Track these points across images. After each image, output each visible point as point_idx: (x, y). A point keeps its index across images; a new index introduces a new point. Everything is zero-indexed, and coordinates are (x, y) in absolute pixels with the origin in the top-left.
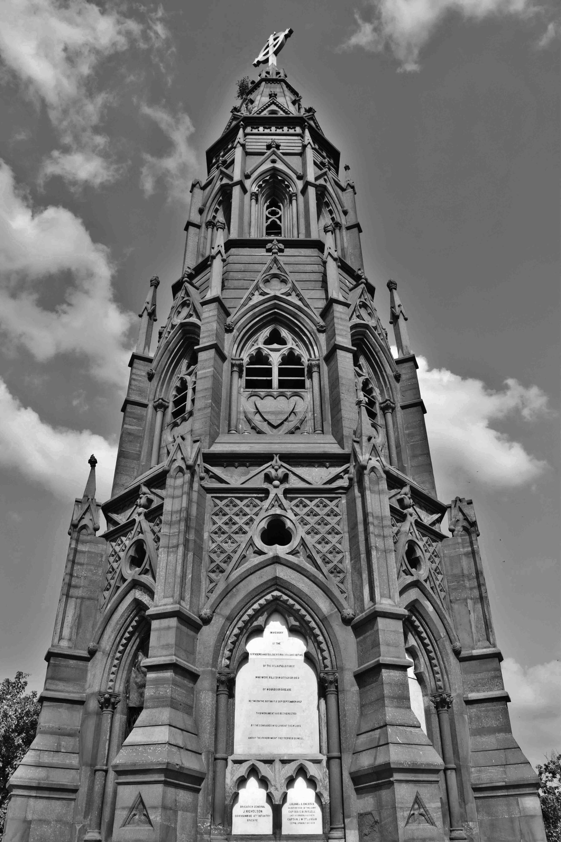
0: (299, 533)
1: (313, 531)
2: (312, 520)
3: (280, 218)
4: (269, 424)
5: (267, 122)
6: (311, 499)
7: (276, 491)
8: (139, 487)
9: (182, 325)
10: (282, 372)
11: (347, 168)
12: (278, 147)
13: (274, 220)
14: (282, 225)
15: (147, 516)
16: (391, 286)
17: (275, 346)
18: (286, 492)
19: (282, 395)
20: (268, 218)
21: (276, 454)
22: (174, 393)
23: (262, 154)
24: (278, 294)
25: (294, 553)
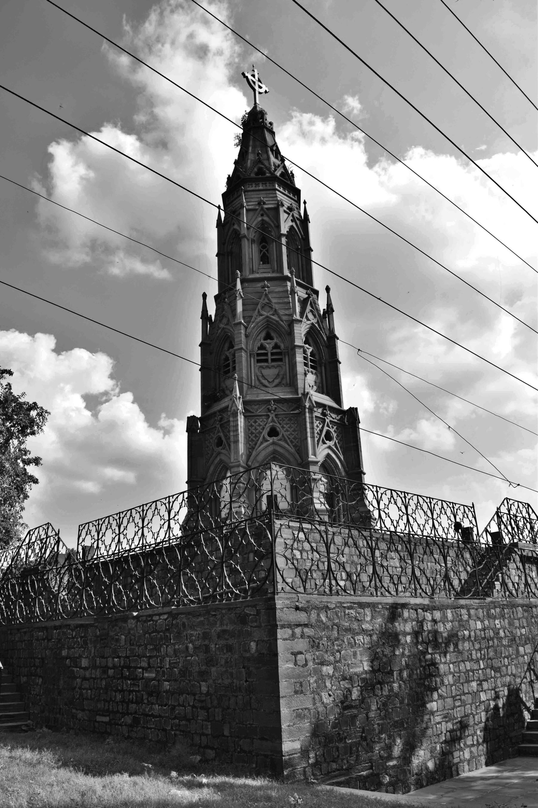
0: (282, 432)
1: (287, 431)
2: (286, 427)
3: (267, 251)
4: (268, 381)
5: (256, 181)
6: (286, 418)
7: (272, 415)
8: (215, 413)
9: (224, 328)
10: (272, 354)
11: (305, 203)
12: (264, 203)
13: (264, 253)
14: (269, 255)
15: (222, 426)
16: (328, 289)
17: (269, 341)
18: (276, 415)
19: (273, 366)
20: (261, 251)
21: (272, 399)
22: (223, 362)
23: (256, 210)
24: (268, 314)
25: (280, 440)
